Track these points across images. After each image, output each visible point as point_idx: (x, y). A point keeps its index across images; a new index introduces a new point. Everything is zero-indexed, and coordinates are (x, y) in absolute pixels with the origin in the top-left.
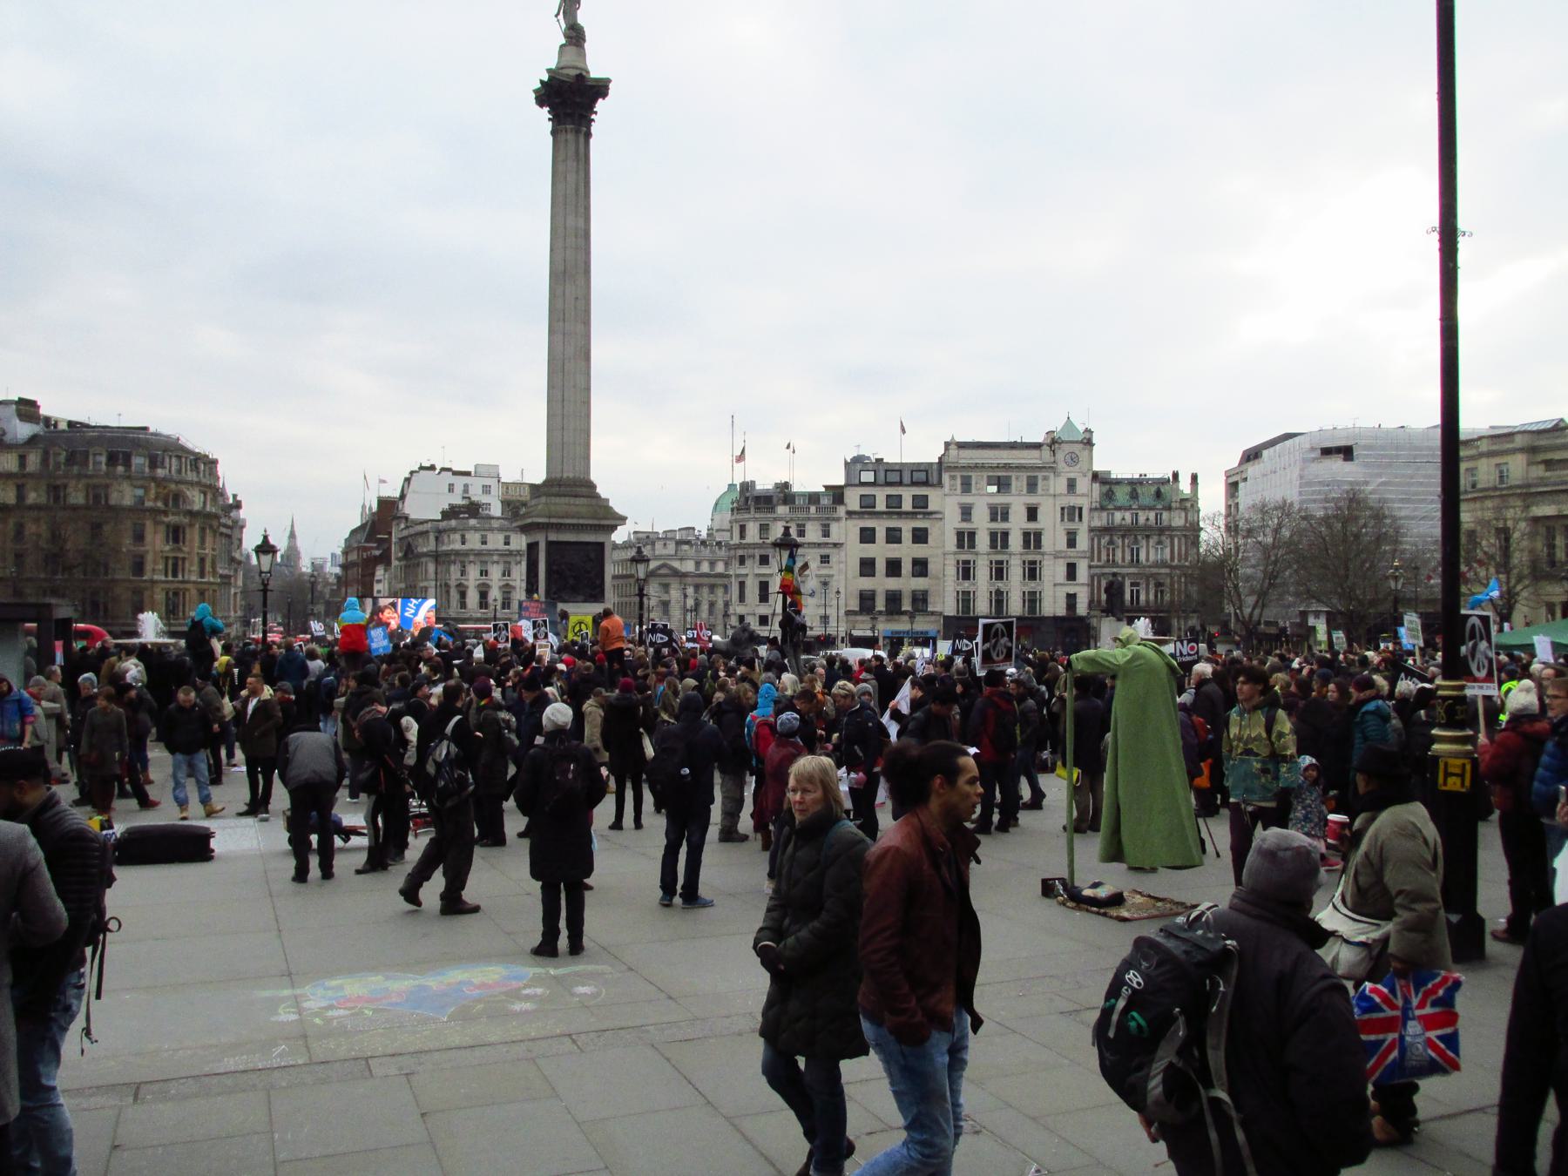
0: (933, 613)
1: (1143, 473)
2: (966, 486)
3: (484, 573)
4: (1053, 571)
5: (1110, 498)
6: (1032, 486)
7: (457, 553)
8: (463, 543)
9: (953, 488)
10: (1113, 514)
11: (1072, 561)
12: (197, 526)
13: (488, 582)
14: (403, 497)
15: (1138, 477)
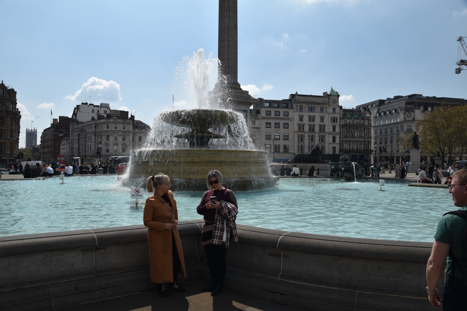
0: (291, 153)
1: (353, 107)
2: (301, 109)
3: (116, 139)
4: (329, 139)
5: (345, 115)
6: (322, 110)
7: (106, 131)
8: (108, 128)
9: (297, 110)
10: (346, 121)
11: (334, 136)
12: (10, 117)
13: (116, 142)
14: (75, 114)
15: (351, 109)
